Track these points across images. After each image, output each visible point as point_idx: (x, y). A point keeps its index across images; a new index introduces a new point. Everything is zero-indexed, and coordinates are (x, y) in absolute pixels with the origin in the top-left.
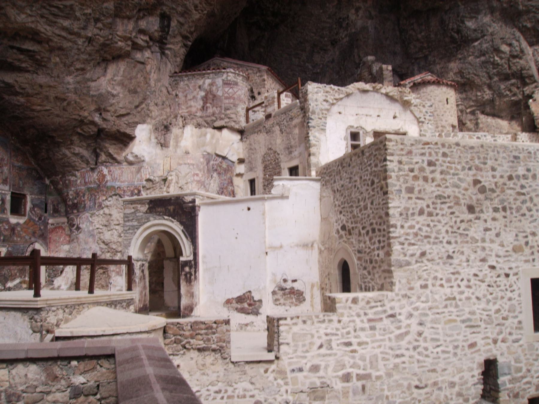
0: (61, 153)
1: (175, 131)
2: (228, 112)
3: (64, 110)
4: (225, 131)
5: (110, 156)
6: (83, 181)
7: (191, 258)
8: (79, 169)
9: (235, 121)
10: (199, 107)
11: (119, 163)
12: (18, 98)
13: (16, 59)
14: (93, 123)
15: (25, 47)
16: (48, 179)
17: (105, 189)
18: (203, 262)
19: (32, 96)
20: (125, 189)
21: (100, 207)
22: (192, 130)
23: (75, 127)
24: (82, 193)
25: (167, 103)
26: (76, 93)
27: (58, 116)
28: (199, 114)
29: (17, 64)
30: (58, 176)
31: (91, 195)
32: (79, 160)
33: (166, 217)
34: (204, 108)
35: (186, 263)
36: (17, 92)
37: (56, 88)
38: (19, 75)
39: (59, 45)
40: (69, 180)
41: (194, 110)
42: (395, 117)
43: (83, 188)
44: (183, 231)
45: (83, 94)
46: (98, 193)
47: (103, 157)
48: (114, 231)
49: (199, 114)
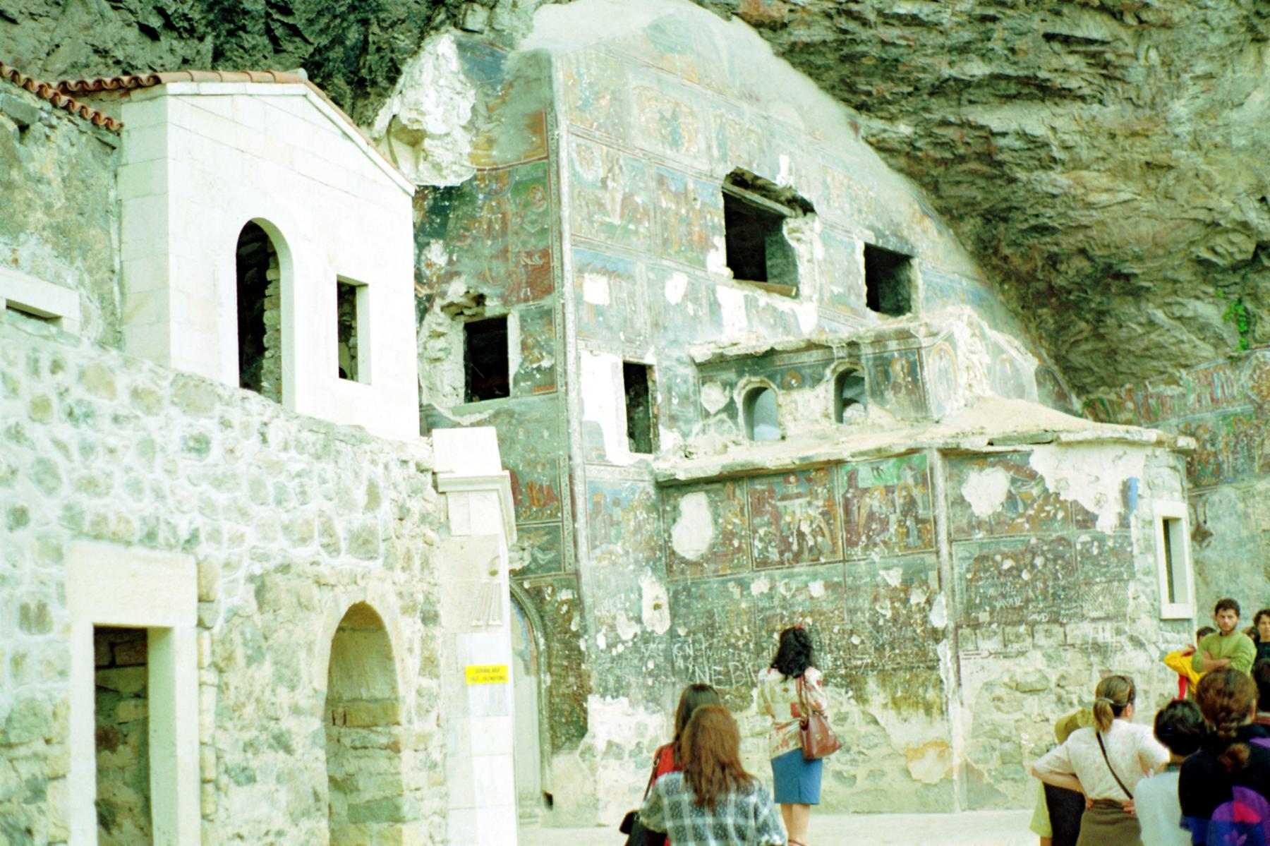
0: (1143, 320)
3: (1169, 197)
6: (1206, 400)
8: (1194, 361)
12: (1052, 174)
13: (1056, 70)
14: (1245, 226)
15: (1079, 33)
16: (1078, 396)
19: (1087, 168)
23: (1192, 243)
24: (1207, 430)
26: (1197, 146)
27: (1151, 216)
29: (1059, 81)
30: (1122, 386)
31: (1237, 437)
32: (1194, 338)
36: (1054, 160)
37: (1147, 137)
38: (1058, 110)
39: (1164, 15)
40: (1160, 397)
43: (1208, 415)
45: (1216, 146)
46: (1258, 427)
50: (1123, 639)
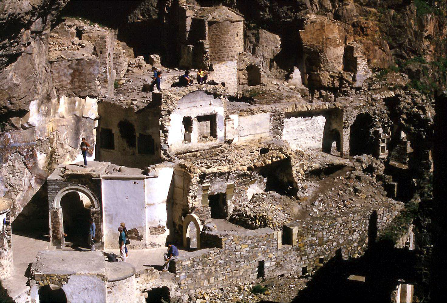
1: (54, 101)
2: (90, 84)
4: (88, 98)
5: (13, 125)
7: (99, 209)
9: (94, 91)
10: (69, 81)
11: (17, 128)
14: (5, 107)
17: (9, 149)
18: (105, 211)
20: (23, 147)
21: (6, 161)
22: (64, 99)
25: (46, 80)
28: (69, 86)
33: (80, 185)
34: (72, 82)
35: (94, 212)
41: (65, 83)
42: (210, 104)
44: (92, 194)
47: (8, 127)
48: (17, 177)
49: (69, 86)
50: (3, 250)
